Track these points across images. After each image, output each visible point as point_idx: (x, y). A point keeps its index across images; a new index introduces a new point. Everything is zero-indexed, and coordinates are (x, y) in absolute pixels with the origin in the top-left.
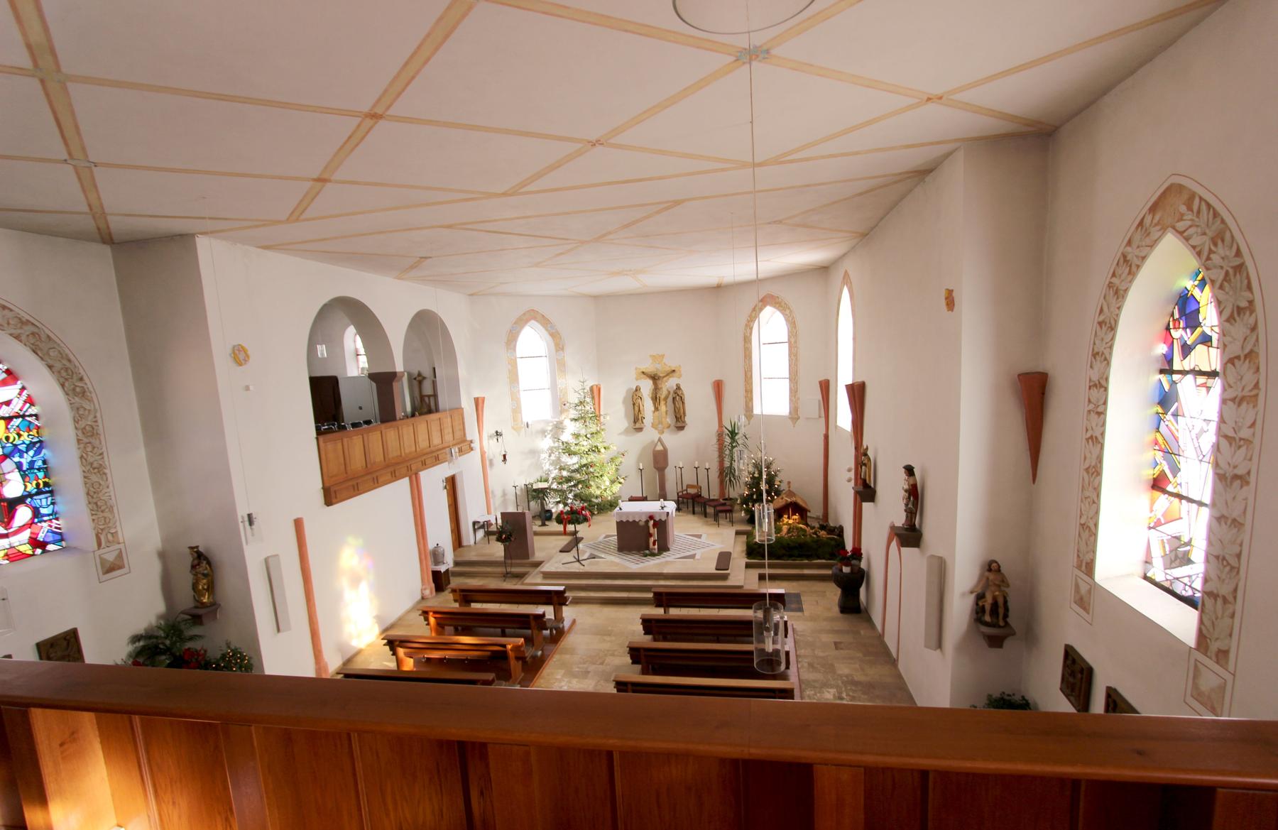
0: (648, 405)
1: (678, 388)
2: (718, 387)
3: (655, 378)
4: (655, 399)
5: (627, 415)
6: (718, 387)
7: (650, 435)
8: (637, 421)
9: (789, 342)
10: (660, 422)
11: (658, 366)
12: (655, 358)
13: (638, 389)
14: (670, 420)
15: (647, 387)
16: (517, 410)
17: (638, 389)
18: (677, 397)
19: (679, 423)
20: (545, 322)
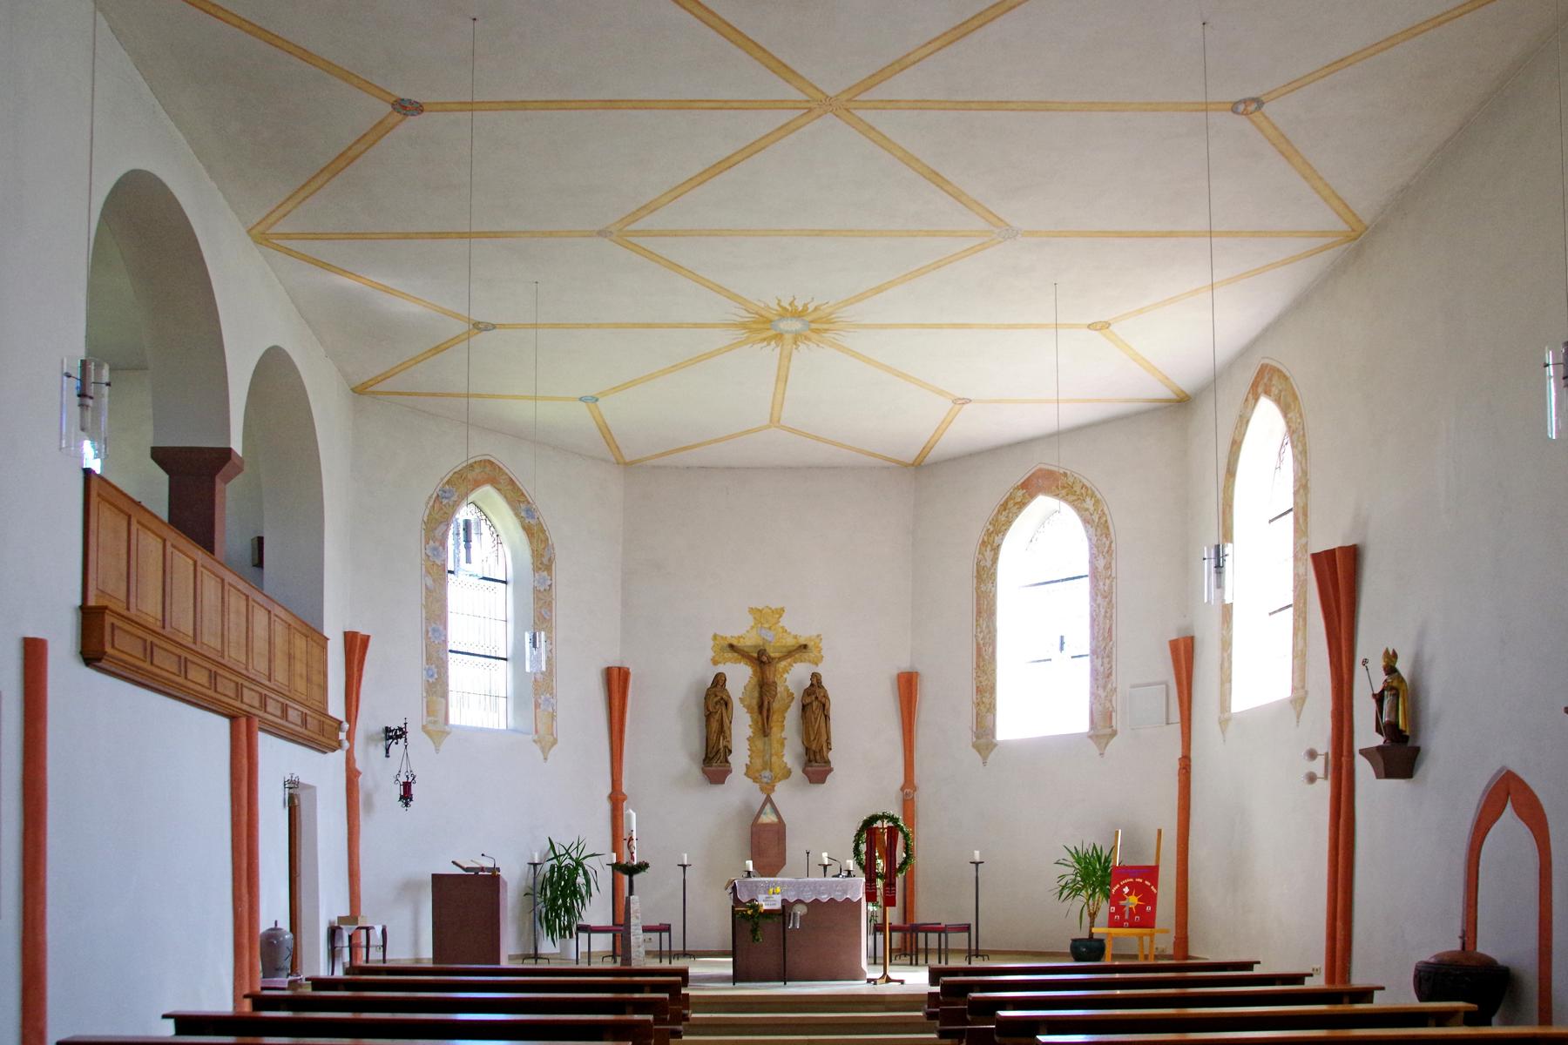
1: (816, 680)
2: (908, 687)
4: (764, 710)
6: (908, 687)
9: (1094, 575)
10: (767, 765)
11: (769, 635)
13: (719, 681)
15: (740, 677)
16: (437, 686)
17: (719, 681)
18: (815, 701)
20: (516, 498)
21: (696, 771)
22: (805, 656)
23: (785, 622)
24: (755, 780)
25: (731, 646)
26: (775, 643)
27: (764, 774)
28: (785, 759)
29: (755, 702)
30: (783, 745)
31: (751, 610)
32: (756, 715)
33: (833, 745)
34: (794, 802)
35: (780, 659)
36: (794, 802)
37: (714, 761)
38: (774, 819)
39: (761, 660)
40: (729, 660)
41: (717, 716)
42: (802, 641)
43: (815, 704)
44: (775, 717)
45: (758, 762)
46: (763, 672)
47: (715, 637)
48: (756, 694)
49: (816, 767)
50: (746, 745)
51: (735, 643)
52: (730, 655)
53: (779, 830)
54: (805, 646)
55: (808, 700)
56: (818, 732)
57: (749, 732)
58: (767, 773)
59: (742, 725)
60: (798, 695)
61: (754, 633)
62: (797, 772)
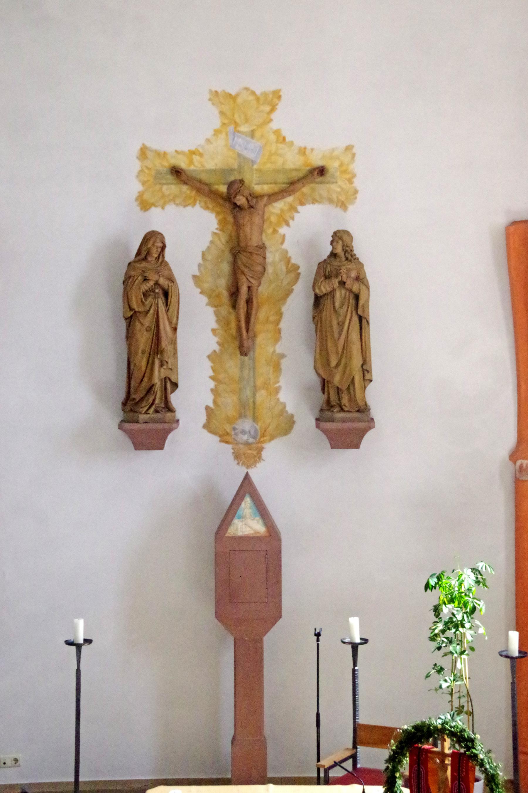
10: (247, 409)
11: (250, 149)
12: (237, 109)
13: (151, 249)
14: (293, 388)
17: (151, 249)
18: (339, 286)
21: (110, 417)
23: (280, 121)
24: (224, 438)
25: (176, 172)
26: (261, 164)
27: (242, 427)
28: (282, 397)
29: (223, 284)
30: (277, 368)
31: (216, 97)
32: (226, 309)
34: (296, 481)
35: (273, 197)
36: (296, 481)
37: (143, 405)
39: (234, 201)
40: (173, 199)
41: (148, 321)
42: (317, 161)
43: (338, 295)
44: (262, 313)
45: (230, 402)
46: (238, 226)
48: (226, 267)
49: (341, 420)
50: (206, 369)
51: (183, 164)
52: (173, 188)
54: (322, 171)
55: (324, 288)
57: (212, 344)
58: (247, 424)
59: (197, 331)
60: (308, 271)
61: (221, 142)
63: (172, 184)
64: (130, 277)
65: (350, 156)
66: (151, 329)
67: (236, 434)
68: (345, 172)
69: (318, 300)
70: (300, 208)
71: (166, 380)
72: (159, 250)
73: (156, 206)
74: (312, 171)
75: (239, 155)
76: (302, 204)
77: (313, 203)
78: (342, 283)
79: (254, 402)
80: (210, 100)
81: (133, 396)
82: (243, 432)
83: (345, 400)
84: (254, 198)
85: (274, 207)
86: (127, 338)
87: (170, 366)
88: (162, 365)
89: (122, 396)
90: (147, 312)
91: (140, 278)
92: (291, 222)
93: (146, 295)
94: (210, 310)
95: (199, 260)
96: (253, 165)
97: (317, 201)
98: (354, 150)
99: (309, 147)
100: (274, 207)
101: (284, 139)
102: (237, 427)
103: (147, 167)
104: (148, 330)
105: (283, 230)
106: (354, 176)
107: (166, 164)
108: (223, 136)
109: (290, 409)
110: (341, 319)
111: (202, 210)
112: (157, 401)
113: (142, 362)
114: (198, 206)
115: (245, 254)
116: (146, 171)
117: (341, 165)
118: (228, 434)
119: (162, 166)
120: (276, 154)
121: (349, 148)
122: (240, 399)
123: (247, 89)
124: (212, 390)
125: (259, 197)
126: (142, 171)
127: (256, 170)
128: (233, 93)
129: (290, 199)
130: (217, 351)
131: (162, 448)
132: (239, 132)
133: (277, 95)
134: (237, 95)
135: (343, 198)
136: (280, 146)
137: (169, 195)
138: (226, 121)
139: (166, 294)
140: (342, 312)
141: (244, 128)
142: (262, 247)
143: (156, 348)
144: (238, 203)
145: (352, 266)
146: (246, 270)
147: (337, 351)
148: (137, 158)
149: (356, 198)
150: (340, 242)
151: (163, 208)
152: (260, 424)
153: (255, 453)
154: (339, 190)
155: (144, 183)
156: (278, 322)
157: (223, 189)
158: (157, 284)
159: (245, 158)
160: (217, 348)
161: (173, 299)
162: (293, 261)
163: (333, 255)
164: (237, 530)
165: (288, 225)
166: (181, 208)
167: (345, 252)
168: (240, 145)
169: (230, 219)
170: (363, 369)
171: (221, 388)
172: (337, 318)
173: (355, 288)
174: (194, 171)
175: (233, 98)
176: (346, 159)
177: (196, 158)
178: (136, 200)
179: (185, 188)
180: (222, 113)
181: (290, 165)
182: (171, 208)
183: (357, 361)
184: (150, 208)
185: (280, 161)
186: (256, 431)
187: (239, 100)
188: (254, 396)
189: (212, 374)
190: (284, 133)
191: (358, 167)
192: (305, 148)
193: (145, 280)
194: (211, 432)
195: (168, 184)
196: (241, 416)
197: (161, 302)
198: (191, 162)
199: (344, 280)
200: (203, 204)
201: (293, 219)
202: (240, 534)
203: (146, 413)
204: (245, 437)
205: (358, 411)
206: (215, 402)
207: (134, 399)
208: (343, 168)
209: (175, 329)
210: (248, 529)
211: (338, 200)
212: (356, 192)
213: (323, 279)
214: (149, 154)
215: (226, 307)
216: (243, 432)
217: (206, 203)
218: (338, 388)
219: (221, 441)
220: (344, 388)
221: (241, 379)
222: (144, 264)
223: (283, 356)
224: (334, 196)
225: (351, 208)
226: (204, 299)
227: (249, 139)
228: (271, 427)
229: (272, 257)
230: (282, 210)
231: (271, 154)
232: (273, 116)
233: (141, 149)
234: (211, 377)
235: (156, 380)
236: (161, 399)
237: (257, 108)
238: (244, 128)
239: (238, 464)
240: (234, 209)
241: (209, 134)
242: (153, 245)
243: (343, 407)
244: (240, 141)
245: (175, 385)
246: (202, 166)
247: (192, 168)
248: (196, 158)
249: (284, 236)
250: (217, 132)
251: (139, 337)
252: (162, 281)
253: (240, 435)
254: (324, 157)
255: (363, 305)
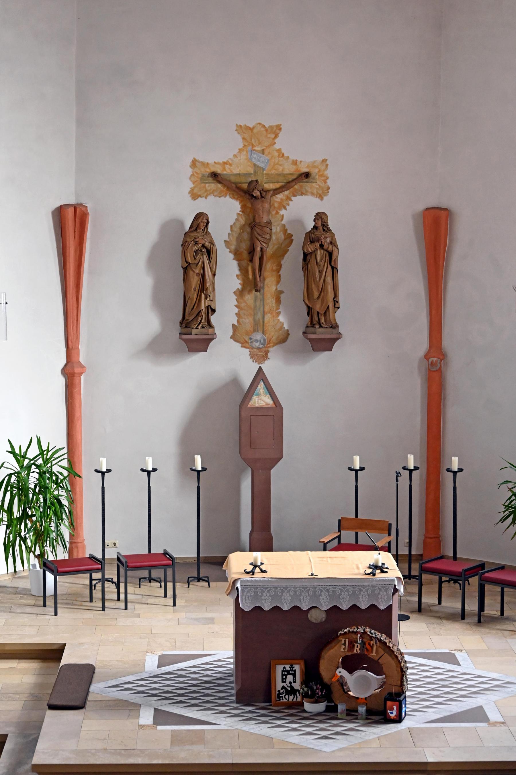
0: (227, 277)
3: (250, 193)
4: (253, 255)
5: (158, 301)
7: (227, 360)
8: (192, 326)
10: (259, 326)
11: (261, 161)
15: (225, 214)
19: (320, 329)
22: (307, 186)
23: (280, 143)
24: (244, 344)
25: (215, 176)
29: (245, 246)
31: (240, 129)
33: (341, 304)
35: (277, 191)
38: (268, 401)
45: (248, 322)
47: (194, 163)
48: (246, 236)
49: (321, 333)
50: (233, 300)
51: (218, 170)
53: (275, 413)
54: (307, 175)
55: (310, 248)
56: (323, 290)
57: (237, 284)
58: (258, 336)
59: (227, 277)
61: (243, 156)
62: (297, 335)
63: (211, 183)
64: (186, 242)
65: (325, 166)
66: (199, 274)
67: (252, 342)
68: (322, 175)
69: (305, 255)
70: (293, 198)
71: (208, 307)
72: (205, 224)
73: (201, 197)
74: (301, 175)
75: (255, 165)
76: (295, 196)
77: (301, 195)
78: (322, 246)
79: (263, 322)
80: (236, 130)
81: (187, 318)
82: (257, 341)
83: (323, 320)
84: (264, 193)
85: (277, 198)
86: (184, 280)
87: (211, 299)
88: (206, 298)
89: (181, 318)
90: (198, 264)
91: (193, 242)
92: (287, 207)
93: (196, 252)
94: (235, 263)
95: (229, 231)
96: (263, 171)
97: (304, 194)
98: (328, 162)
99: (299, 160)
100: (277, 198)
101: (283, 154)
102: (252, 337)
103: (196, 172)
104: (198, 274)
105: (282, 212)
106: (328, 178)
107: (208, 170)
108: (245, 153)
109: (286, 326)
110: (321, 269)
111: (231, 199)
112: (203, 321)
113: (194, 295)
114: (228, 196)
115: (259, 227)
116: (196, 175)
117: (319, 172)
118: (246, 342)
119: (206, 172)
120: (278, 164)
121: (324, 161)
122: (254, 320)
123: (260, 124)
124: (236, 314)
125: (267, 191)
126: (193, 175)
127: (265, 174)
128: (251, 126)
129: (287, 193)
130: (240, 288)
131: (206, 351)
132: (254, 150)
133: (279, 128)
134: (254, 128)
135: (320, 192)
136: (281, 159)
137: (210, 189)
138: (247, 144)
139: (209, 252)
140: (322, 264)
141: (258, 148)
142: (269, 223)
143: (203, 287)
144: (255, 195)
145: (328, 235)
146: (260, 238)
147: (318, 289)
148: (190, 167)
149: (328, 192)
150: (320, 219)
151: (206, 198)
152: (267, 335)
153: (263, 354)
154: (318, 187)
155: (194, 183)
156: (278, 271)
157: (245, 186)
158: (203, 246)
159: (258, 167)
160: (240, 287)
161: (213, 256)
162: (288, 232)
163: (315, 228)
164: (255, 402)
165: (285, 209)
166: (217, 198)
167: (323, 226)
168: (255, 159)
169: (249, 205)
170: (334, 301)
171: (242, 313)
172: (319, 268)
173: (330, 248)
174: (226, 174)
175: (251, 129)
176: (323, 168)
177: (227, 167)
178: (189, 193)
179: (219, 186)
180: (244, 139)
181: (286, 171)
182: (211, 198)
183: (331, 295)
184: (197, 198)
185: (281, 168)
186: (264, 340)
187: (255, 131)
188: (263, 318)
189: (236, 303)
190: (283, 151)
191: (329, 172)
192: (297, 160)
193: (196, 243)
194: (235, 341)
195: (209, 183)
196: (255, 330)
197: (206, 258)
198: (224, 169)
199: (323, 243)
200: (231, 196)
201: (289, 205)
202: (257, 405)
203: (196, 328)
204: (257, 344)
205: (331, 327)
206: (238, 321)
207: (188, 320)
208: (321, 173)
209: (214, 275)
210: (262, 402)
211: (318, 193)
212: (329, 188)
213: (309, 243)
214: (197, 164)
215: (246, 261)
216: (257, 341)
217: (233, 194)
218: (318, 312)
219: (242, 347)
220: (323, 313)
221: (255, 307)
222: (195, 233)
223: (282, 292)
224: (315, 191)
225: (325, 198)
226: (232, 256)
227: (260, 154)
228: (274, 338)
229: (276, 229)
230: (281, 199)
231: (275, 164)
232: (276, 141)
233: (193, 161)
234: (236, 306)
235: (203, 307)
236: (205, 319)
237: (266, 136)
238: (258, 148)
239: (253, 361)
240: (252, 198)
241: (236, 151)
242: (202, 222)
243: (322, 325)
244: (255, 156)
245: (214, 311)
246: (231, 171)
247: (225, 172)
248: (227, 167)
249: (283, 216)
250: (241, 151)
251: (192, 280)
252: (207, 244)
253: (254, 343)
254: (308, 167)
255: (335, 260)
